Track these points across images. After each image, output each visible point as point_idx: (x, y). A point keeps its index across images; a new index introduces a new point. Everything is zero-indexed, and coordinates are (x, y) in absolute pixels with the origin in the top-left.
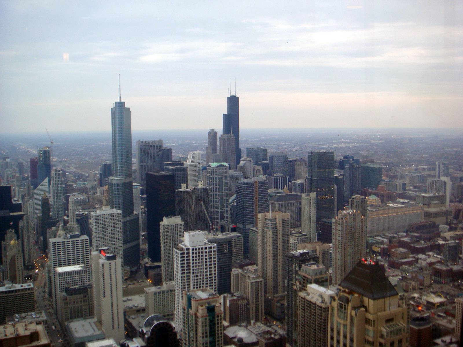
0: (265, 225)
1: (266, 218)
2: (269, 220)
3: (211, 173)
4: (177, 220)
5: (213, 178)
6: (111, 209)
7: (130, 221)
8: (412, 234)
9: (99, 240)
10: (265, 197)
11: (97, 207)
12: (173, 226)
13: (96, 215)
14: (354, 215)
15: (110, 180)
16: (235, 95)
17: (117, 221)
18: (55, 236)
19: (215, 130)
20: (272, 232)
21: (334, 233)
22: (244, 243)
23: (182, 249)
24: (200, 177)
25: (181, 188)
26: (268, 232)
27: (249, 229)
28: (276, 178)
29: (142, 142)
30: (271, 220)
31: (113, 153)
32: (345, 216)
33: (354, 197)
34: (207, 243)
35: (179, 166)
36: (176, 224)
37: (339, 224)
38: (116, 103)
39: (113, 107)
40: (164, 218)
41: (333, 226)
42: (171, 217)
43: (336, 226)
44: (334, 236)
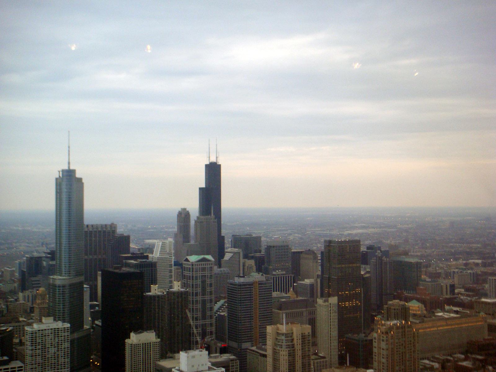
0: (277, 343)
1: (278, 333)
2: (283, 334)
3: (190, 269)
4: (150, 337)
5: (193, 276)
6: (55, 322)
7: (78, 339)
8: (474, 356)
9: (36, 368)
10: (268, 303)
11: (21, 319)
12: (144, 345)
13: (33, 331)
15: (51, 280)
16: (215, 161)
17: (63, 339)
19: (187, 210)
20: (287, 353)
21: (376, 353)
22: (240, 369)
24: (171, 275)
25: (150, 291)
26: (281, 353)
27: (247, 349)
28: (281, 277)
29: (87, 226)
30: (286, 335)
31: (56, 241)
32: (391, 328)
33: (390, 302)
34: (211, 368)
35: (144, 260)
36: (149, 342)
37: (383, 341)
38: (63, 171)
39: (57, 176)
40: (132, 334)
41: (374, 343)
42: (141, 333)
43: (379, 343)
44: (376, 358)
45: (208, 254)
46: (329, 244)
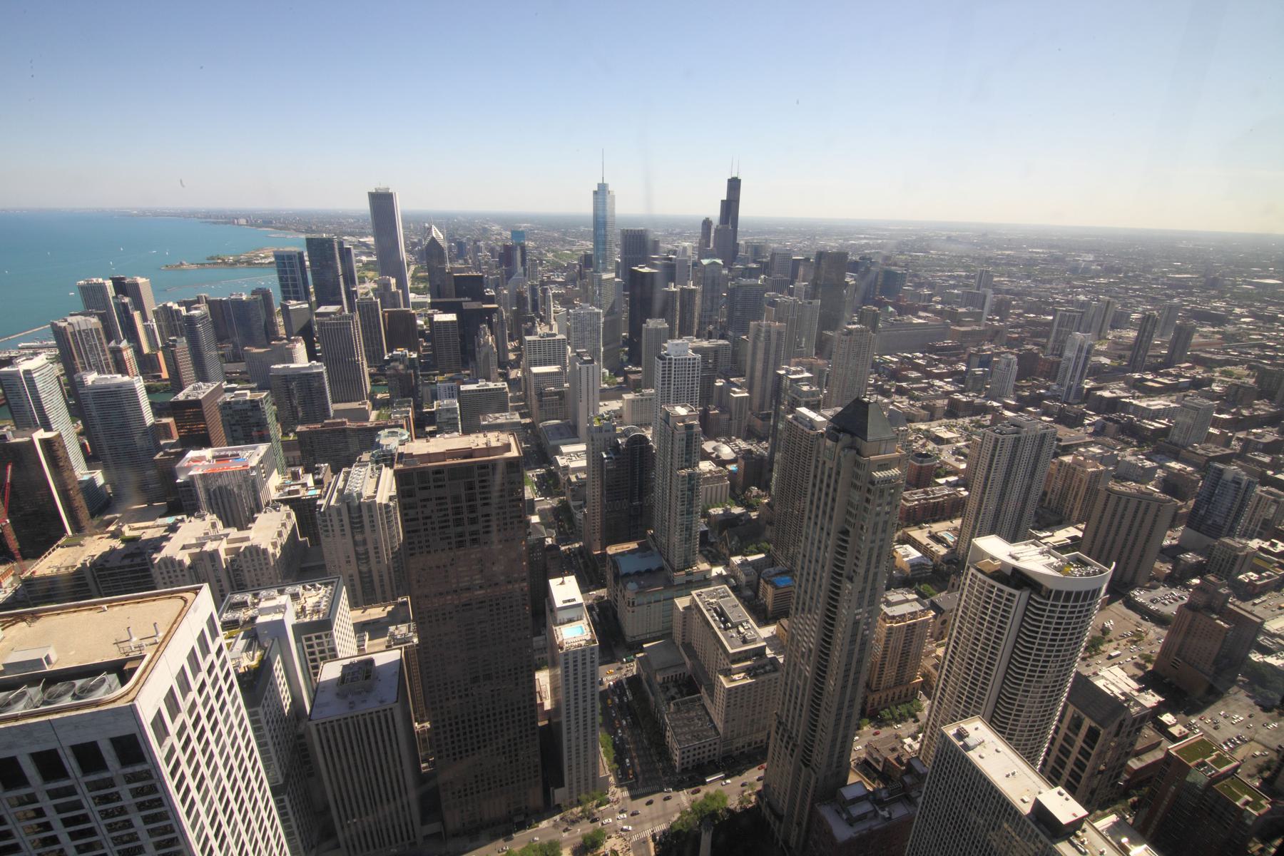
14: (861, 331)
18: (530, 334)
23: (665, 359)
45: (719, 258)
46: (821, 255)
